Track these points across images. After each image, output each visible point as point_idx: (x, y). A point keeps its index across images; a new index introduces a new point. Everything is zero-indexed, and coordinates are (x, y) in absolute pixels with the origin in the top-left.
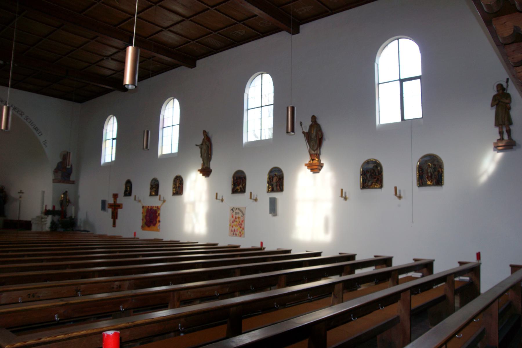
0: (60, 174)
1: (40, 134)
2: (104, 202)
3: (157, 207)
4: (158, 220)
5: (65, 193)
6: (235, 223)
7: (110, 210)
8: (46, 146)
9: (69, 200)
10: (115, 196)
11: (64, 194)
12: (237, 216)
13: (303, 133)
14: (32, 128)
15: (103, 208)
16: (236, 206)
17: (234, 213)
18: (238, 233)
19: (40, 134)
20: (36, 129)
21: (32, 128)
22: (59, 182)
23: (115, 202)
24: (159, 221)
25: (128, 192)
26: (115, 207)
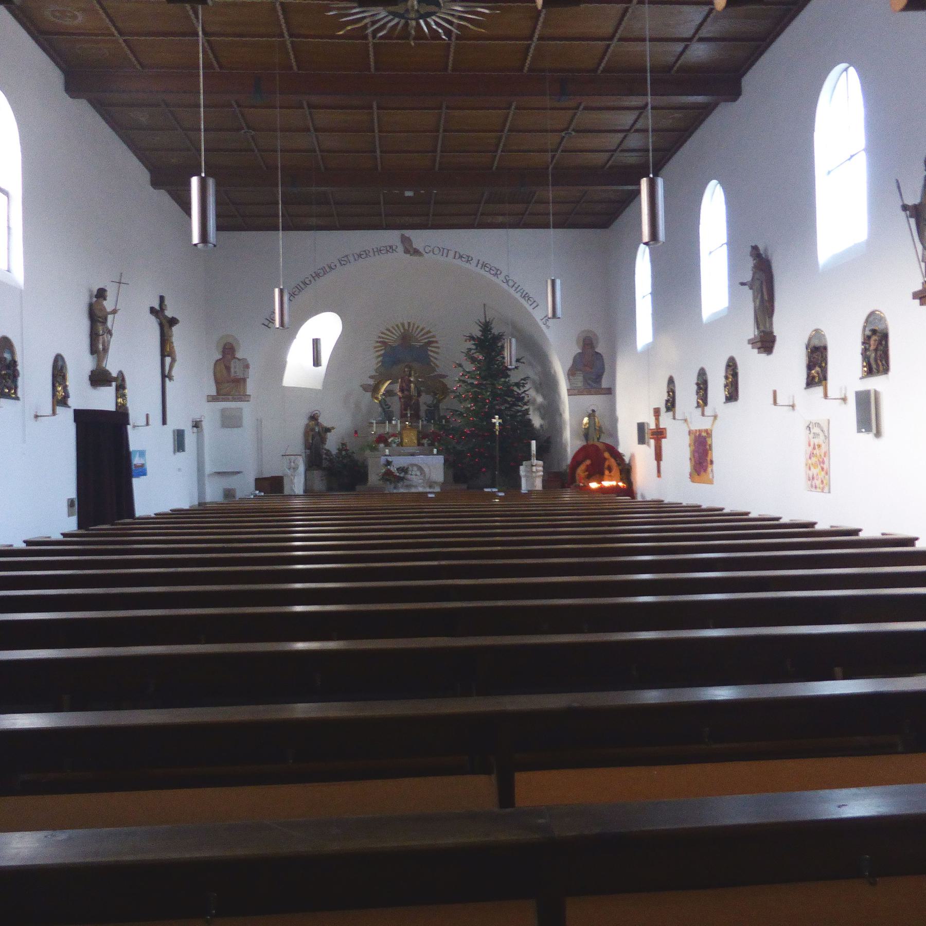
0: (579, 378)
1: (535, 305)
2: (641, 427)
3: (706, 431)
4: (709, 459)
5: (592, 415)
6: (814, 459)
7: (652, 442)
8: (548, 327)
9: (600, 427)
10: (657, 412)
11: (589, 416)
12: (816, 441)
13: (905, 208)
14: (518, 296)
15: (642, 440)
16: (814, 419)
17: (812, 435)
18: (818, 483)
19: (535, 305)
20: (526, 296)
21: (518, 296)
22: (581, 393)
23: (657, 425)
24: (712, 462)
25: (671, 405)
26: (659, 434)
